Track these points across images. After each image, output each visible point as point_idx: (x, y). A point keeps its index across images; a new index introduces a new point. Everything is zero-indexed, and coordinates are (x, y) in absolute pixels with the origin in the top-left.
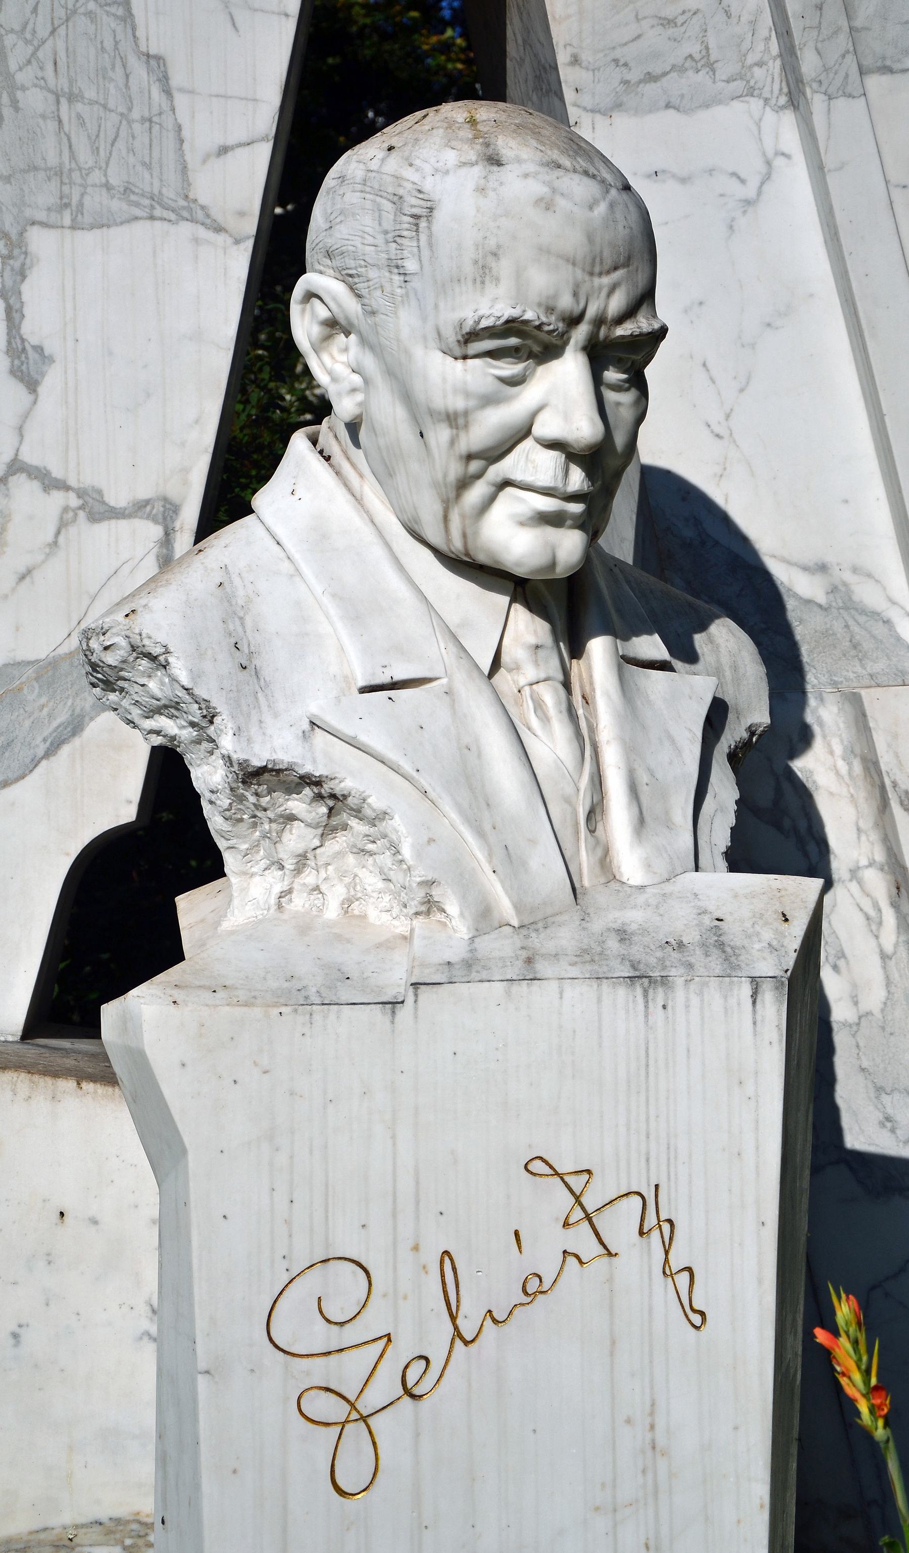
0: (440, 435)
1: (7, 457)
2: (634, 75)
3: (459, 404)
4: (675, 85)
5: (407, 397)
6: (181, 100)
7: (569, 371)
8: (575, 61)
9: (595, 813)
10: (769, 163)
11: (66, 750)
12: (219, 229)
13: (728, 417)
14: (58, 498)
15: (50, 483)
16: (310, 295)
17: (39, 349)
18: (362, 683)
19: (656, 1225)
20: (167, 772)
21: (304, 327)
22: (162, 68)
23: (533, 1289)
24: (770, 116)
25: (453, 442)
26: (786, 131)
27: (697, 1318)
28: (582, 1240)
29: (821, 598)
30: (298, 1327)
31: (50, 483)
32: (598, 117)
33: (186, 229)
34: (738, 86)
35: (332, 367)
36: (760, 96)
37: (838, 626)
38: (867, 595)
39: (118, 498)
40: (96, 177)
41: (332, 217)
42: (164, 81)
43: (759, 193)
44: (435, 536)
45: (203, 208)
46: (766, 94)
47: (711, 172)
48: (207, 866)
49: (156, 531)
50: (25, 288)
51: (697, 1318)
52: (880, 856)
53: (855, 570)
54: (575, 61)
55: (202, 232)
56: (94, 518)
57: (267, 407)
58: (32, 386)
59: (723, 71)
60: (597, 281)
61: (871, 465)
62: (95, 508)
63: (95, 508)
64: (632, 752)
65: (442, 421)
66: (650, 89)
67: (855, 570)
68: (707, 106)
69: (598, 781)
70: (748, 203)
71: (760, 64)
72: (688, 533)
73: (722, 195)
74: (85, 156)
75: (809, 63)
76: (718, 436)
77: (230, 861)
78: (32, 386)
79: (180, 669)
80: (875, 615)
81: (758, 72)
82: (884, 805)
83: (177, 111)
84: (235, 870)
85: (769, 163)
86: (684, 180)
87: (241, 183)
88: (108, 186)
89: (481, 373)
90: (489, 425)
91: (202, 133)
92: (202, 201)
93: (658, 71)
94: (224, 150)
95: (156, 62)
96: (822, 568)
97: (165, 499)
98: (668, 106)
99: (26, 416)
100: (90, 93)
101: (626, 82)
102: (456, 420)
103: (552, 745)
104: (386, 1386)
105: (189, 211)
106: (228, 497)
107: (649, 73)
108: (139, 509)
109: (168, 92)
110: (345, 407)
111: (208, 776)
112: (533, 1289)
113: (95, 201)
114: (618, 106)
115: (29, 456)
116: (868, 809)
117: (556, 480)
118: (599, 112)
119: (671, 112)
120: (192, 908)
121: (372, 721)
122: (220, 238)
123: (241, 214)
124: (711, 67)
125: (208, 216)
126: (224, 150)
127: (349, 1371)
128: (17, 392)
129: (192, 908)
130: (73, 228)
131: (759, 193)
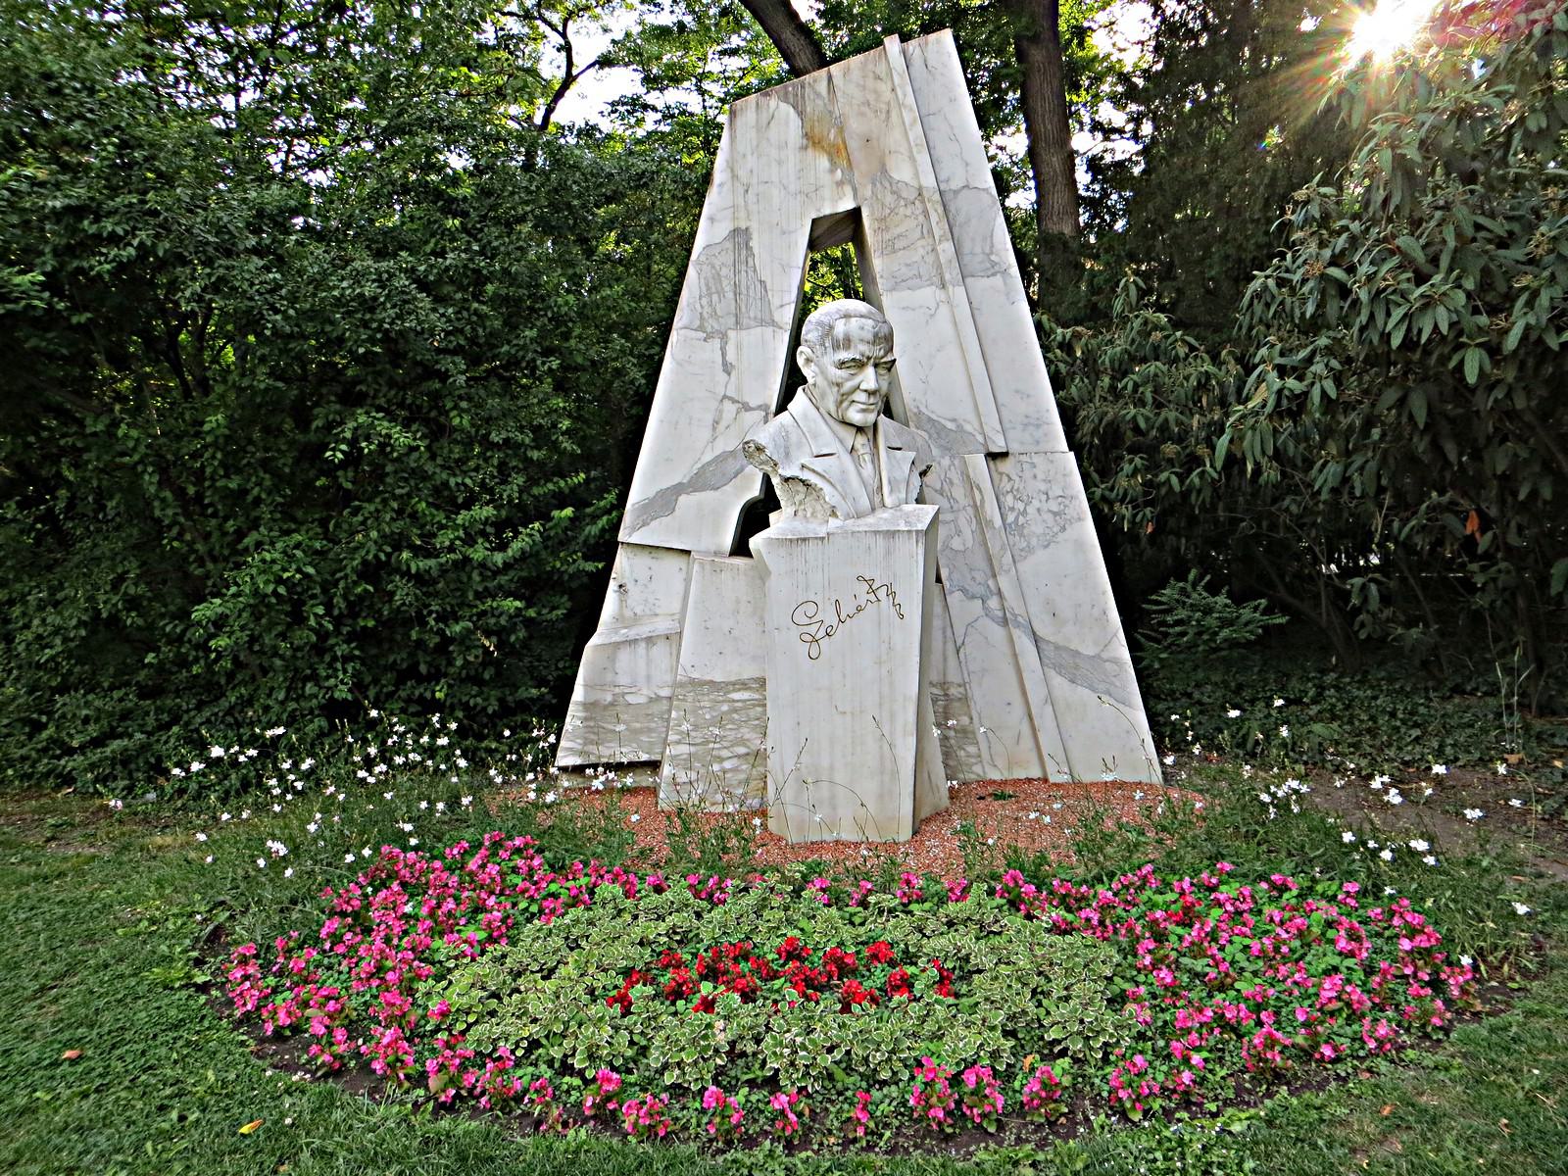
4: (910, 283)
7: (870, 371)
9: (881, 487)
19: (891, 594)
20: (767, 481)
21: (800, 361)
23: (859, 609)
26: (940, 295)
27: (902, 617)
28: (872, 597)
30: (800, 618)
31: (734, 401)
35: (806, 371)
38: (968, 428)
39: (752, 404)
48: (777, 506)
51: (902, 617)
57: (794, 379)
62: (747, 408)
63: (747, 408)
64: (889, 471)
75: (947, 277)
87: (787, 316)
89: (843, 373)
90: (848, 386)
91: (775, 302)
96: (954, 420)
103: (868, 469)
104: (822, 633)
106: (782, 407)
108: (759, 407)
110: (810, 381)
111: (775, 481)
112: (859, 609)
113: (745, 321)
120: (773, 517)
121: (819, 465)
127: (813, 629)
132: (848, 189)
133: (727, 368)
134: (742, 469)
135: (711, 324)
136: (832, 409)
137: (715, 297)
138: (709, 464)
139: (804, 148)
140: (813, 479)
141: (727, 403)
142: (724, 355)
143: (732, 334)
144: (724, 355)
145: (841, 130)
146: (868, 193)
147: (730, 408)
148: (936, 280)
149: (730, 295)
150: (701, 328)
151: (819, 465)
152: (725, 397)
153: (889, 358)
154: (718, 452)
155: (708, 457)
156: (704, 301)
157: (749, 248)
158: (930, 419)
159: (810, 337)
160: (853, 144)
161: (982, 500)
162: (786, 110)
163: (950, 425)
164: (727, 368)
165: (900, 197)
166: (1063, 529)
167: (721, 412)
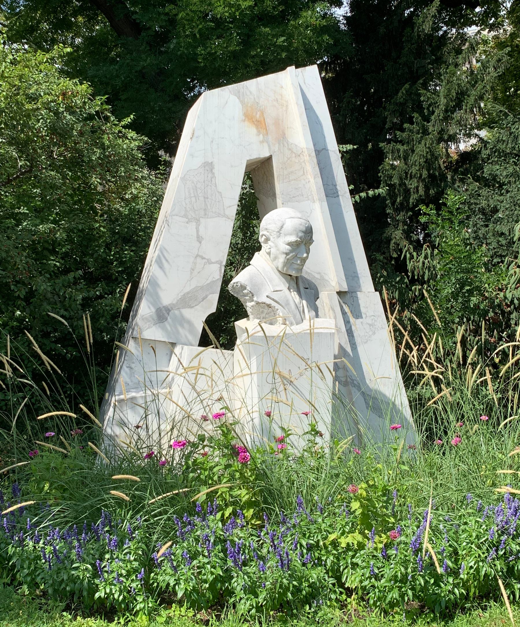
14: (204, 261)
15: (203, 258)
16: (262, 235)
39: (213, 261)
42: (221, 196)
44: (280, 269)
49: (219, 266)
56: (209, 264)
58: (200, 243)
62: (209, 262)
63: (209, 262)
69: (303, 306)
74: (209, 207)
77: (251, 317)
78: (200, 243)
94: (230, 207)
95: (220, 193)
96: (319, 273)
105: (225, 216)
108: (216, 262)
112: (301, 375)
115: (200, 254)
126: (230, 207)
128: (198, 243)
129: (240, 324)
132: (265, 145)
133: (199, 239)
134: (206, 297)
136: (280, 266)
137: (193, 199)
138: (188, 293)
139: (244, 121)
140: (273, 304)
141: (199, 260)
142: (198, 231)
144: (198, 231)
145: (262, 113)
146: (276, 149)
149: (202, 199)
150: (185, 216)
151: (275, 296)
152: (198, 256)
154: (193, 287)
155: (187, 289)
157: (213, 174)
160: (269, 121)
162: (233, 100)
163: (317, 276)
164: (199, 239)
165: (292, 152)
166: (374, 333)
167: (195, 263)
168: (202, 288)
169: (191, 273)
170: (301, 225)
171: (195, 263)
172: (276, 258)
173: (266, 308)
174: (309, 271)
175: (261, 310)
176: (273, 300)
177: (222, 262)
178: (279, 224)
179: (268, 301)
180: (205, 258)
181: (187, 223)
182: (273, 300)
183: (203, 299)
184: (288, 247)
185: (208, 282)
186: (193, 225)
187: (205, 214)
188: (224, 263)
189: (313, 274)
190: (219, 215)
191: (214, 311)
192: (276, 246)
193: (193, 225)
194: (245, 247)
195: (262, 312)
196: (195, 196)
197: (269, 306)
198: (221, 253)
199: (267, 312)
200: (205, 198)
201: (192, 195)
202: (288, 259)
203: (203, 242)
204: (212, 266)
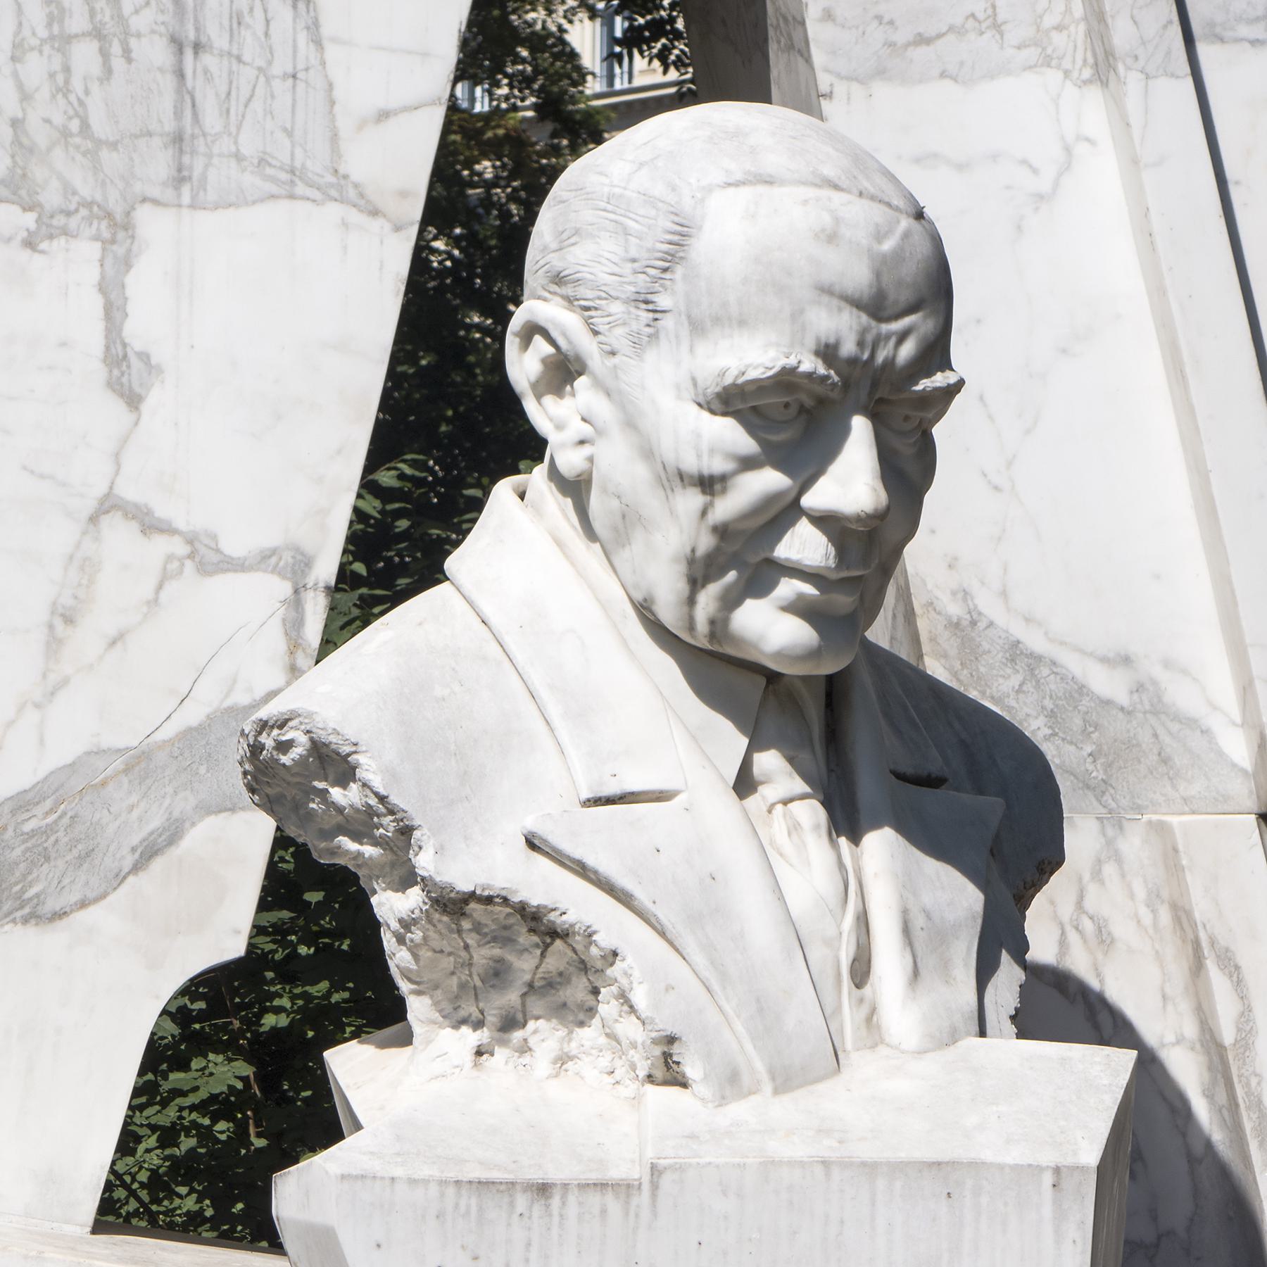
0: (692, 500)
1: (100, 489)
2: (901, 37)
3: (718, 465)
5: (648, 453)
6: (332, 52)
8: (828, 16)
10: (1068, 150)
11: (158, 864)
12: (375, 212)
13: (1009, 464)
14: (162, 546)
15: (150, 525)
16: (533, 330)
17: (145, 357)
18: (585, 795)
22: (312, 14)
24: (1070, 90)
25: (704, 513)
26: (1091, 111)
29: (1123, 698)
31: (150, 525)
32: (855, 86)
33: (334, 211)
34: (1031, 54)
36: (1058, 67)
37: (1145, 737)
38: (1182, 696)
39: (234, 546)
40: (226, 145)
41: (564, 236)
43: (1056, 184)
45: (356, 186)
46: (1067, 64)
47: (994, 157)
49: (284, 588)
50: (130, 280)
52: (1190, 1029)
53: (1167, 664)
54: (828, 16)
55: (355, 216)
58: (133, 401)
59: (1014, 34)
60: (886, 328)
61: (1189, 530)
62: (205, 557)
63: (205, 557)
65: (695, 485)
66: (920, 54)
67: (1167, 664)
68: (991, 76)
69: (863, 920)
70: (1040, 197)
71: (1059, 28)
72: (955, 609)
73: (1008, 187)
74: (211, 119)
75: (1122, 34)
76: (996, 488)
78: (133, 401)
79: (370, 768)
80: (1191, 723)
81: (1059, 39)
82: (1197, 968)
83: (328, 65)
84: (421, 1017)
85: (1068, 150)
86: (961, 167)
88: (238, 157)
92: (355, 176)
93: (931, 32)
94: (384, 115)
96: (1126, 661)
97: (297, 550)
98: (943, 75)
99: (124, 441)
100: (217, 36)
101: (891, 45)
102: (709, 484)
107: (920, 34)
108: (264, 560)
109: (318, 43)
114: (881, 73)
115: (129, 491)
116: (1178, 971)
117: (827, 559)
118: (857, 80)
119: (947, 83)
122: (377, 224)
123: (404, 194)
124: (997, 27)
125: (362, 195)
126: (384, 115)
128: (116, 409)
129: (352, 1065)
130: (193, 206)
131: (1056, 184)
133: (126, 373)
134: (172, 834)
135: (63, 175)
136: (667, 589)
137: (85, 56)
141: (119, 536)
142: (114, 313)
143: (154, 226)
144: (114, 313)
147: (127, 555)
148: (1072, 42)
149: (155, 52)
151: (597, 838)
152: (109, 505)
153: (940, 379)
154: (62, 752)
156: (36, 68)
158: (1015, 651)
159: (578, 258)
161: (1245, 1016)
163: (1107, 684)
164: (126, 373)
167: (84, 567)
168: (139, 763)
169: (54, 644)
170: (831, 237)
171: (84, 567)
172: (629, 520)
173: (525, 938)
174: (1035, 642)
175: (483, 955)
176: (581, 870)
177: (302, 563)
178: (652, 234)
179: (540, 884)
180: (165, 529)
181: (30, 244)
182: (581, 870)
183: (148, 853)
184: (731, 435)
185: (193, 714)
186: (80, 260)
187: (180, 178)
188: (327, 568)
189: (1074, 664)
190: (291, 183)
191: (234, 947)
192: (631, 423)
193: (80, 260)
194: (447, 433)
195: (498, 974)
196: (98, 34)
197: (540, 925)
198: (318, 479)
199: (529, 962)
200: (177, 44)
201: (77, 22)
202: (723, 531)
203: (153, 400)
204: (223, 584)
